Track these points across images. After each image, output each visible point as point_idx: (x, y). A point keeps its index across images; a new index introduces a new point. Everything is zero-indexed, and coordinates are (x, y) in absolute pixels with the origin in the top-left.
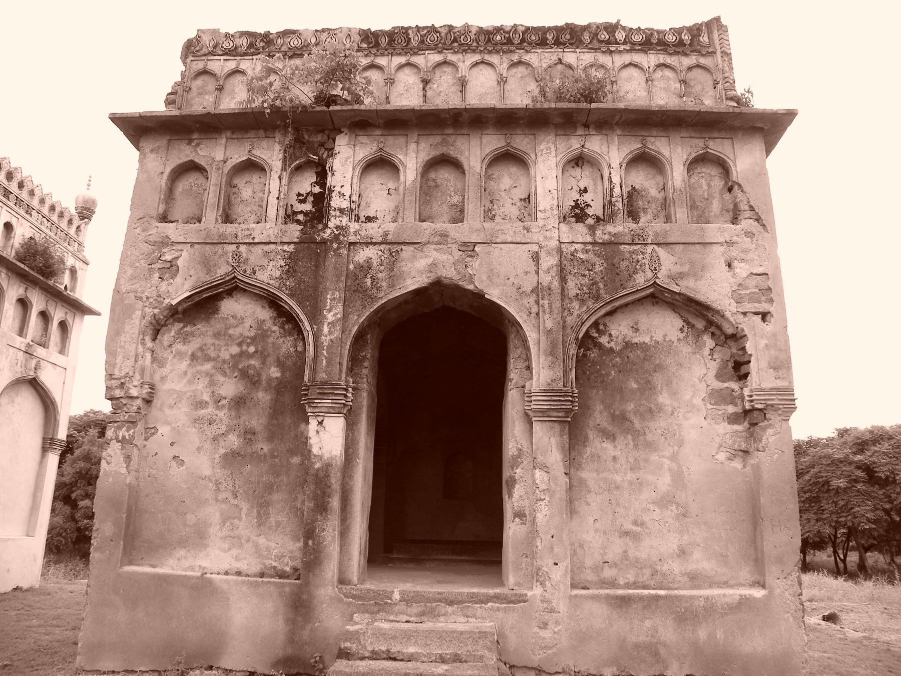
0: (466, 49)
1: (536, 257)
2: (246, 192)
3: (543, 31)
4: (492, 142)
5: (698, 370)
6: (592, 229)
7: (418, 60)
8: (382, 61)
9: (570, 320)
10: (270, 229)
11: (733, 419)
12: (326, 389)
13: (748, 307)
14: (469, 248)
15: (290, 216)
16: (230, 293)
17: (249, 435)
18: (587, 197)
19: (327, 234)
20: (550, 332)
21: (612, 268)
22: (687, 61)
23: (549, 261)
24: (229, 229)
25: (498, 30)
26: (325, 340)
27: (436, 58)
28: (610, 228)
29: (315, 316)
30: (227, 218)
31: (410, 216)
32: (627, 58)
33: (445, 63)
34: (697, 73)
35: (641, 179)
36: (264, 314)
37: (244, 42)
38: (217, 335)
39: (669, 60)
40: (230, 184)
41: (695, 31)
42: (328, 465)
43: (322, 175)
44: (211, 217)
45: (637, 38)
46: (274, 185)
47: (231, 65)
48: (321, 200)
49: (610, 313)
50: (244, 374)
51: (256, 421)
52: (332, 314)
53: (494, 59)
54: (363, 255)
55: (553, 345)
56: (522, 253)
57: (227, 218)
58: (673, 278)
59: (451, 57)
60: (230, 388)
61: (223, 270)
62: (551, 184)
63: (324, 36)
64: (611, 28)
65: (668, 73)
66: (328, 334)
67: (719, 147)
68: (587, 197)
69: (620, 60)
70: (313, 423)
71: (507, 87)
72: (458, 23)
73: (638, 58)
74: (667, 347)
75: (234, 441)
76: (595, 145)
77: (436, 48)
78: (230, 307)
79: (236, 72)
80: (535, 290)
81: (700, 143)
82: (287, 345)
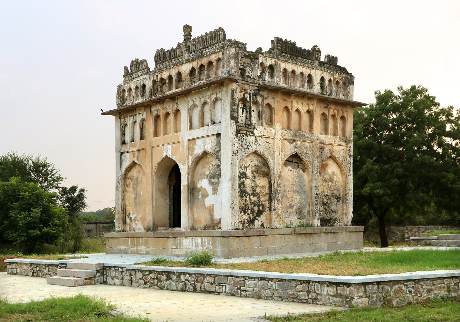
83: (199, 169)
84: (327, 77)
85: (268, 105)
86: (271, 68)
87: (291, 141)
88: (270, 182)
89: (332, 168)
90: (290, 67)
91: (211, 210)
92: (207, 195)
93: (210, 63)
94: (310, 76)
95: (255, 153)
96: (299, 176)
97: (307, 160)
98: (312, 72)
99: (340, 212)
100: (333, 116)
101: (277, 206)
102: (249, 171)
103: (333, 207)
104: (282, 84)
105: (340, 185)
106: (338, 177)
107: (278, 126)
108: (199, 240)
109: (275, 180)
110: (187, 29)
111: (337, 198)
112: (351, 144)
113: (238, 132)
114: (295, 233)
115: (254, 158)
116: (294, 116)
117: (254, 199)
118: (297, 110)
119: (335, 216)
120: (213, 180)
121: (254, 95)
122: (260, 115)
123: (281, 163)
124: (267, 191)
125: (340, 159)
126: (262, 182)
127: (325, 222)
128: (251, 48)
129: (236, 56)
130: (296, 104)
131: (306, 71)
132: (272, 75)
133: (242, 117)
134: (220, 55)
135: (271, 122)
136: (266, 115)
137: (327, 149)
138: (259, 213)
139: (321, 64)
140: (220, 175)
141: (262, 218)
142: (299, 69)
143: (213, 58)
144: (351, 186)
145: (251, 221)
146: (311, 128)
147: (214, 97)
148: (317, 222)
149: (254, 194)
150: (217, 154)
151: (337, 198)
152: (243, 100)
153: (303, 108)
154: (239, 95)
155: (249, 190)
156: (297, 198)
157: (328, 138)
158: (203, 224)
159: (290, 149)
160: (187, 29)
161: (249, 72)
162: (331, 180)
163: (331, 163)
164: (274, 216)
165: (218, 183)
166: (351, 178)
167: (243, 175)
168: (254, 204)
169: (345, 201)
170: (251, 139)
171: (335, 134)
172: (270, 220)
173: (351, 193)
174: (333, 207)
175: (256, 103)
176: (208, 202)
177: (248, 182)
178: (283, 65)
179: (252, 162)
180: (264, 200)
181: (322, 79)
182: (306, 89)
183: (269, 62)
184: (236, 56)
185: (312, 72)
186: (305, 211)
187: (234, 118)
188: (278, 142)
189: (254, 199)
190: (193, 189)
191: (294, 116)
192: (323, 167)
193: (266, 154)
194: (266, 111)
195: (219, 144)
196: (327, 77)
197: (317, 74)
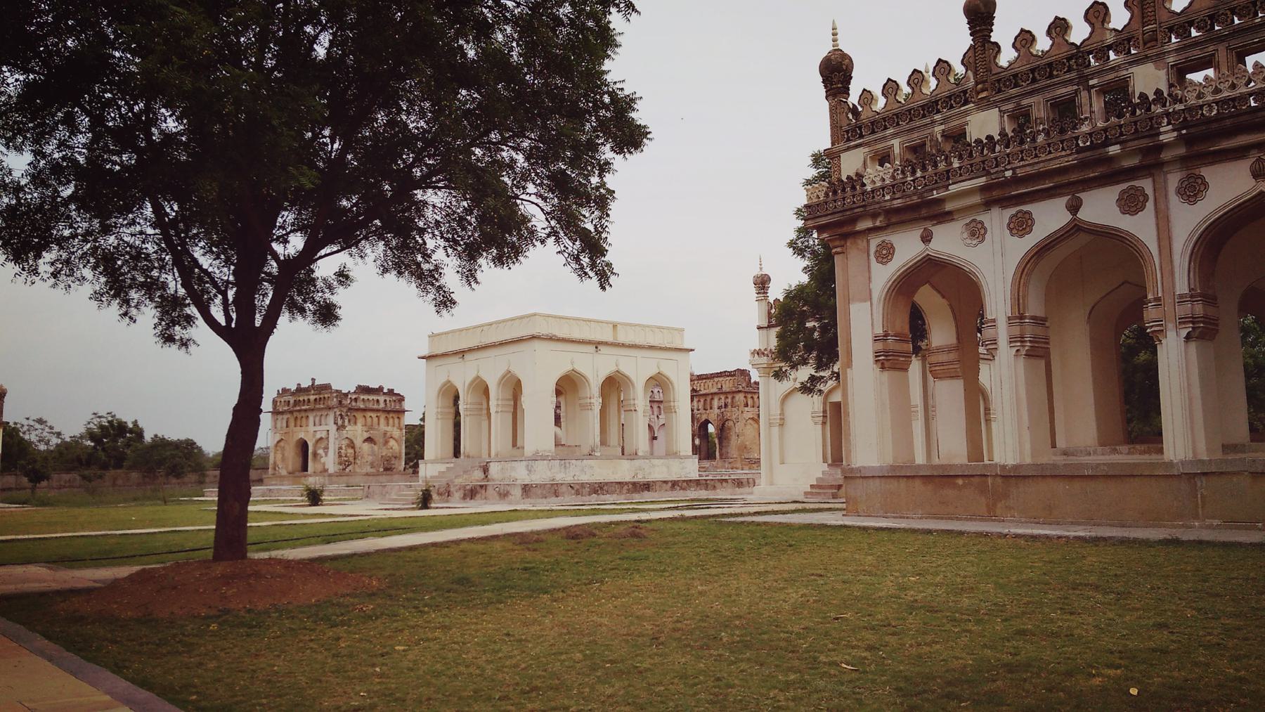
84: (388, 399)
90: (366, 397)
97: (376, 439)
98: (379, 398)
102: (343, 446)
105: (397, 451)
109: (357, 450)
111: (395, 458)
119: (393, 466)
122: (349, 421)
123: (362, 439)
126: (350, 451)
127: (386, 469)
129: (337, 397)
133: (340, 422)
135: (355, 423)
137: (388, 434)
139: (384, 394)
141: (350, 468)
144: (404, 451)
145: (344, 469)
146: (379, 424)
148: (382, 470)
151: (395, 458)
152: (341, 415)
154: (338, 413)
156: (370, 458)
159: (366, 435)
161: (344, 402)
167: (341, 448)
172: (354, 468)
177: (342, 451)
178: (362, 397)
179: (345, 442)
181: (385, 401)
183: (354, 397)
184: (337, 397)
185: (379, 398)
186: (375, 464)
188: (360, 431)
189: (346, 459)
192: (386, 442)
193: (352, 438)
194: (352, 418)
196: (388, 399)
197: (382, 399)
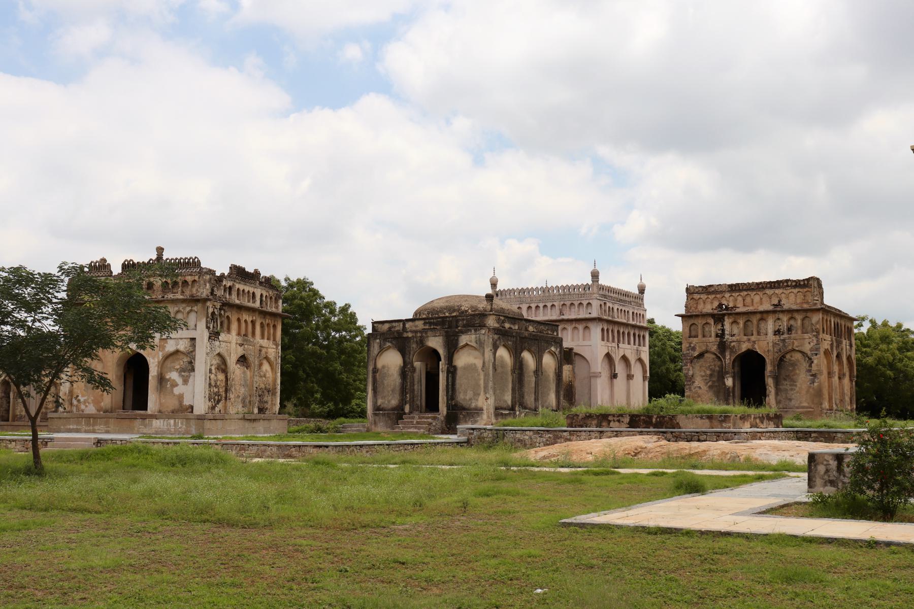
0: (753, 290)
1: (768, 343)
2: (707, 329)
3: (770, 283)
4: (759, 316)
5: (805, 365)
6: (780, 337)
7: (742, 294)
8: (733, 294)
9: (775, 357)
10: (713, 339)
11: (812, 375)
12: (727, 373)
13: (813, 352)
14: (754, 342)
15: (717, 336)
16: (706, 352)
17: (714, 382)
18: (781, 327)
19: (725, 340)
20: (771, 360)
21: (784, 345)
22: (805, 290)
23: (771, 344)
24: (704, 339)
25: (761, 283)
26: (727, 363)
27: (746, 293)
28: (783, 336)
29: (725, 358)
30: (704, 336)
31: (742, 334)
32: (790, 291)
33: (748, 294)
34: (808, 293)
35: (792, 322)
36: (714, 356)
37: (700, 289)
38: (705, 362)
39: (801, 290)
40: (703, 328)
41: (808, 280)
42: (729, 388)
43: (723, 326)
44: (700, 336)
45: (794, 284)
46: (713, 329)
47: (699, 297)
48: (723, 330)
49: (787, 353)
50: (711, 369)
51: (714, 379)
52: (728, 357)
53: (759, 293)
54: (732, 344)
55: (771, 362)
56: (765, 343)
57: (704, 336)
58: (797, 347)
59: (750, 293)
60: (708, 372)
61: (704, 348)
62: (771, 326)
63: (719, 287)
64: (787, 281)
65: (801, 293)
66: (727, 362)
67: (809, 314)
68: (781, 327)
69: (788, 291)
70: (726, 380)
71: (763, 300)
72: (751, 282)
73: (793, 290)
74: (798, 361)
75: (710, 383)
76: (781, 316)
77: (746, 290)
78: (706, 355)
79: (700, 298)
80: (768, 351)
81: (805, 314)
82: (719, 363)
83: (169, 363)
84: (265, 294)
85: (228, 317)
86: (230, 288)
87: (241, 345)
88: (226, 377)
89: (266, 367)
90: (241, 287)
91: (181, 397)
92: (177, 385)
93: (185, 283)
94: (254, 293)
95: (219, 355)
96: (244, 373)
97: (251, 359)
98: (255, 290)
99: (270, 403)
100: (268, 325)
101: (232, 396)
102: (213, 368)
103: (265, 399)
104: (237, 302)
105: (270, 380)
106: (269, 374)
107: (234, 332)
108: (172, 421)
110: (160, 250)
112: (280, 347)
113: (209, 338)
114: (244, 419)
115: (217, 358)
116: (243, 325)
117: (216, 390)
118: (246, 321)
120: (183, 374)
121: (220, 309)
123: (235, 362)
124: (224, 384)
125: (272, 359)
126: (221, 377)
127: (261, 410)
128: (218, 274)
130: (246, 317)
131: (251, 290)
132: (230, 294)
134: (196, 278)
135: (229, 330)
136: (225, 325)
137: (264, 350)
138: (219, 401)
139: (261, 283)
140: (193, 370)
141: (220, 406)
142: (247, 288)
143: (189, 279)
144: (279, 381)
145: (213, 408)
147: (188, 309)
148: (256, 411)
149: (216, 386)
150: (191, 354)
152: (213, 313)
153: (249, 319)
154: (211, 310)
155: (213, 383)
156: (242, 390)
157: (264, 343)
158: (171, 408)
159: (240, 351)
160: (160, 250)
162: (265, 376)
163: (265, 362)
164: (229, 404)
165: (189, 377)
166: (279, 374)
168: (216, 394)
169: (274, 394)
170: (217, 343)
171: (268, 339)
172: (225, 407)
173: (279, 387)
174: (265, 399)
175: (220, 315)
176: (176, 391)
177: (213, 376)
178: (237, 286)
179: (216, 361)
180: (222, 390)
181: (262, 295)
182: (251, 304)
183: (229, 284)
185: (255, 290)
187: (208, 328)
188: (233, 345)
189: (216, 390)
190: (161, 379)
191: (243, 325)
192: (261, 365)
193: (225, 355)
194: (226, 322)
195: (194, 346)
197: (258, 292)
